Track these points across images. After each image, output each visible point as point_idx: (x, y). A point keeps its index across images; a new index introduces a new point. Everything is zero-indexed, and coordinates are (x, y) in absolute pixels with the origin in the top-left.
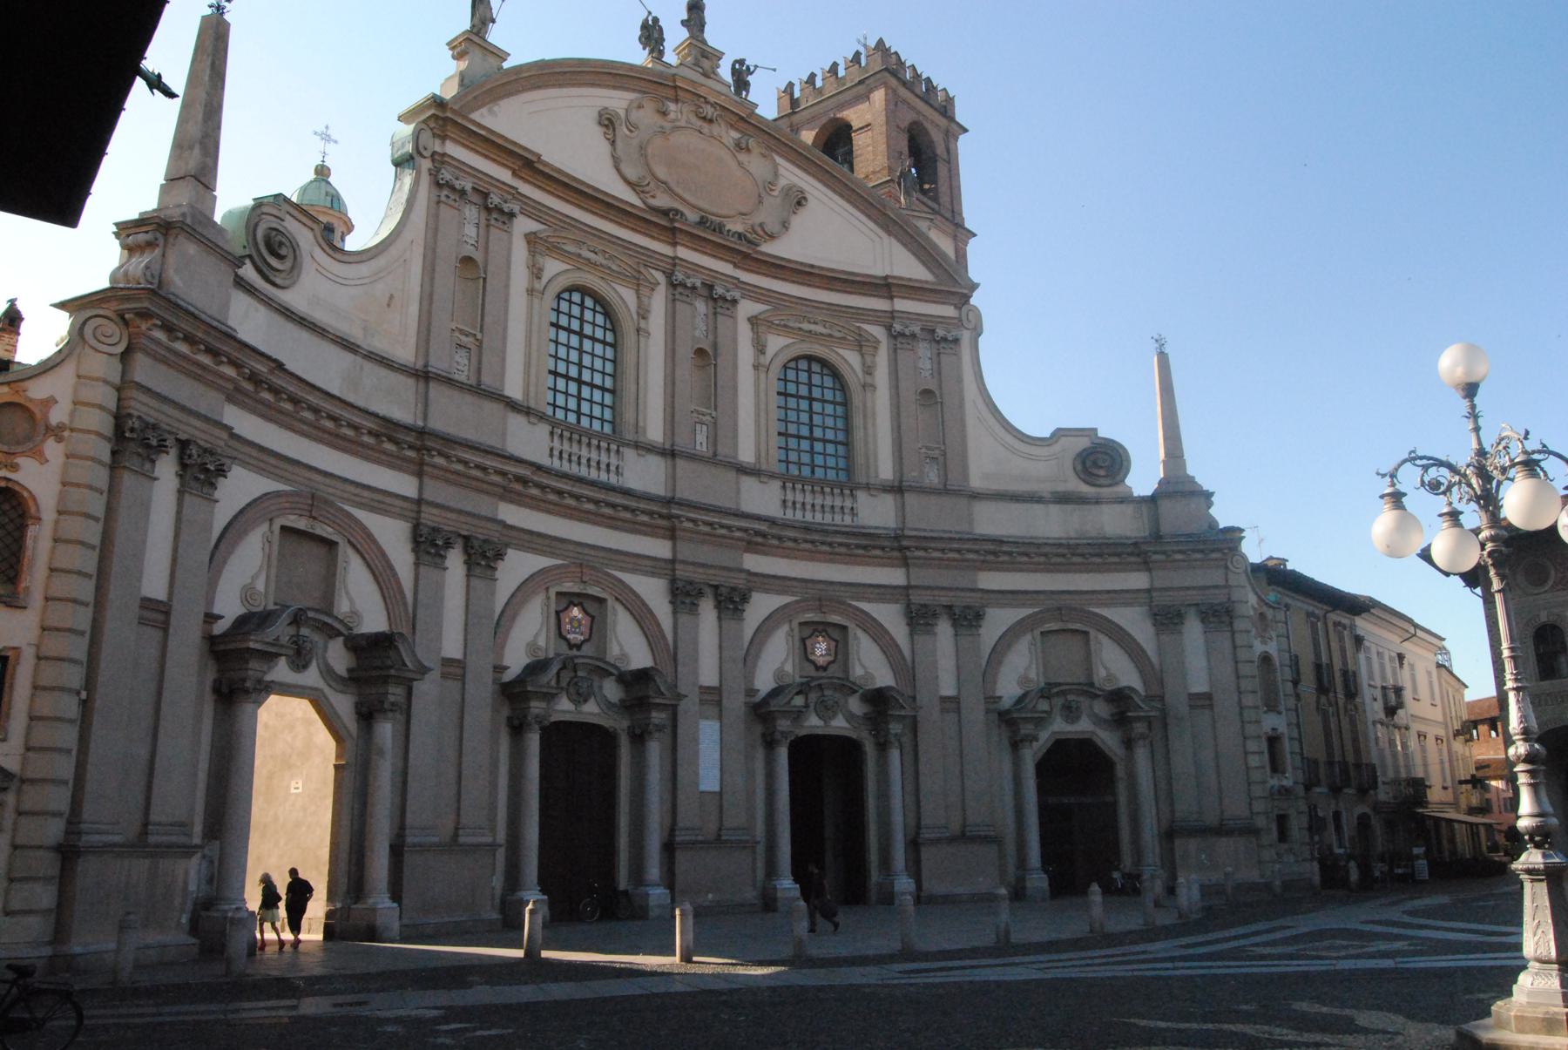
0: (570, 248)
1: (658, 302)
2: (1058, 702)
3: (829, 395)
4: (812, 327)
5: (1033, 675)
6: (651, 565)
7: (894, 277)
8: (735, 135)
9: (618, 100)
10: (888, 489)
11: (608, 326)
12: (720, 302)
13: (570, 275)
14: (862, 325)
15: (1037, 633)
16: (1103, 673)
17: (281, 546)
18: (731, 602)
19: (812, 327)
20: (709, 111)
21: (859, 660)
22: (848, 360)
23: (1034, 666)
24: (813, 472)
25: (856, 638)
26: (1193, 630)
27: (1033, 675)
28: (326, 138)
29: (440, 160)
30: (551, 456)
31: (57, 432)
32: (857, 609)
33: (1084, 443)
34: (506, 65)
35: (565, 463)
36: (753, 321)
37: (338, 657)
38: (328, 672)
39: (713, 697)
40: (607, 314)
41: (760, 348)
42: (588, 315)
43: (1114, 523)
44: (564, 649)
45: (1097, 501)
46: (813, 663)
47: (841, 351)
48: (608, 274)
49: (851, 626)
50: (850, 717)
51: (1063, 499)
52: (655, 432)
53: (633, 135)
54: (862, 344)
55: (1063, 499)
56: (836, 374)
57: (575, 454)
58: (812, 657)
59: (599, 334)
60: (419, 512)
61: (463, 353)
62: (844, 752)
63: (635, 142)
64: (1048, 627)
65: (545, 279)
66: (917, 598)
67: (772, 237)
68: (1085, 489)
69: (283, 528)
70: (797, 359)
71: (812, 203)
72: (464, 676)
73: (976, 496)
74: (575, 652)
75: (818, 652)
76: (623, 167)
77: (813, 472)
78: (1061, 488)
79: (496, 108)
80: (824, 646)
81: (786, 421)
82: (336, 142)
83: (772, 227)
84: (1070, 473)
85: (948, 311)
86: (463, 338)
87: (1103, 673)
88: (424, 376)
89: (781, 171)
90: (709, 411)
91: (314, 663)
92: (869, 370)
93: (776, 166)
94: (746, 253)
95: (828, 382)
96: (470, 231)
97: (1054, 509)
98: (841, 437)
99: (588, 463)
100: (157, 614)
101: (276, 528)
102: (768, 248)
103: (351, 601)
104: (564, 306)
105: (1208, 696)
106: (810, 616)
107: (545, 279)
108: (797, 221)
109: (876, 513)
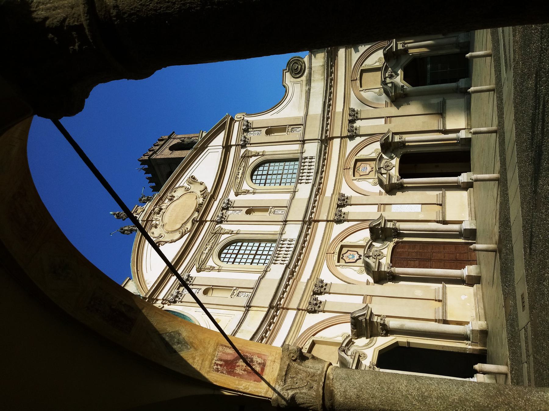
0: (204, 257)
1: (225, 227)
2: (388, 80)
3: (266, 168)
4: (240, 174)
7: (223, 144)
8: (167, 200)
11: (235, 244)
14: (240, 156)
18: (343, 202)
19: (240, 174)
20: (157, 209)
24: (295, 173)
30: (283, 264)
36: (237, 194)
42: (230, 251)
48: (215, 244)
52: (277, 228)
53: (163, 236)
54: (246, 157)
55: (309, 81)
57: (283, 255)
59: (238, 248)
60: (302, 310)
61: (240, 294)
63: (166, 234)
65: (215, 266)
67: (206, 188)
70: (252, 180)
71: (195, 174)
72: (370, 296)
73: (307, 114)
76: (175, 238)
77: (295, 173)
78: (304, 83)
83: (202, 188)
87: (377, 64)
89: (181, 185)
90: (270, 209)
91: (364, 351)
93: (179, 187)
95: (261, 168)
99: (286, 252)
104: (226, 260)
107: (215, 266)
109: (312, 149)
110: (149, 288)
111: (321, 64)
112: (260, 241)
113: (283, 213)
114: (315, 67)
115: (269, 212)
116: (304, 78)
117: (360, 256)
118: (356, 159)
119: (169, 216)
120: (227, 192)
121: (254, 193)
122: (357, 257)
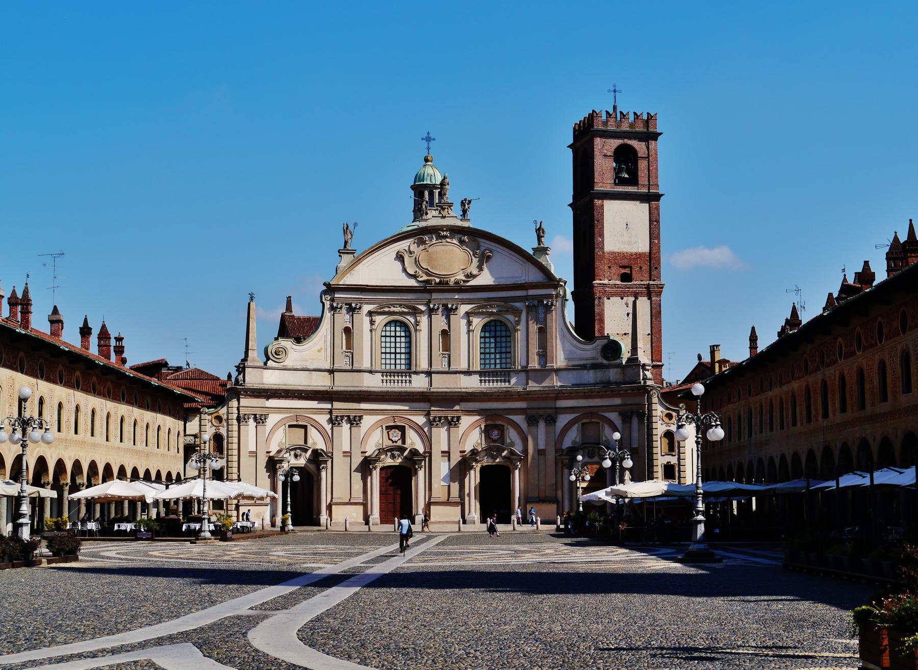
5: (578, 440)
9: (403, 245)
13: (387, 318)
15: (580, 423)
16: (604, 439)
17: (289, 430)
21: (509, 436)
23: (578, 437)
25: (507, 428)
27: (578, 440)
28: (428, 139)
30: (383, 382)
32: (507, 418)
33: (605, 341)
35: (385, 384)
43: (613, 374)
44: (390, 443)
45: (608, 367)
46: (492, 439)
47: (507, 316)
49: (506, 425)
51: (595, 367)
52: (424, 365)
55: (595, 367)
56: (506, 325)
58: (492, 437)
64: (585, 421)
65: (376, 324)
68: (605, 362)
69: (289, 425)
74: (395, 444)
75: (494, 435)
77: (495, 366)
78: (594, 361)
79: (352, 272)
80: (496, 432)
81: (485, 348)
82: (434, 139)
83: (475, 272)
84: (599, 355)
86: (346, 353)
87: (604, 439)
88: (331, 372)
89: (482, 244)
97: (592, 372)
98: (508, 350)
100: (254, 454)
101: (287, 426)
102: (473, 282)
103: (313, 440)
105: (636, 449)
110: (340, 283)
111: (611, 379)
112: (409, 353)
113: (443, 366)
114: (609, 372)
115: (443, 353)
116: (601, 360)
117: (396, 442)
118: (504, 426)
119: (436, 252)
120: (465, 301)
121: (469, 331)
122: (394, 439)
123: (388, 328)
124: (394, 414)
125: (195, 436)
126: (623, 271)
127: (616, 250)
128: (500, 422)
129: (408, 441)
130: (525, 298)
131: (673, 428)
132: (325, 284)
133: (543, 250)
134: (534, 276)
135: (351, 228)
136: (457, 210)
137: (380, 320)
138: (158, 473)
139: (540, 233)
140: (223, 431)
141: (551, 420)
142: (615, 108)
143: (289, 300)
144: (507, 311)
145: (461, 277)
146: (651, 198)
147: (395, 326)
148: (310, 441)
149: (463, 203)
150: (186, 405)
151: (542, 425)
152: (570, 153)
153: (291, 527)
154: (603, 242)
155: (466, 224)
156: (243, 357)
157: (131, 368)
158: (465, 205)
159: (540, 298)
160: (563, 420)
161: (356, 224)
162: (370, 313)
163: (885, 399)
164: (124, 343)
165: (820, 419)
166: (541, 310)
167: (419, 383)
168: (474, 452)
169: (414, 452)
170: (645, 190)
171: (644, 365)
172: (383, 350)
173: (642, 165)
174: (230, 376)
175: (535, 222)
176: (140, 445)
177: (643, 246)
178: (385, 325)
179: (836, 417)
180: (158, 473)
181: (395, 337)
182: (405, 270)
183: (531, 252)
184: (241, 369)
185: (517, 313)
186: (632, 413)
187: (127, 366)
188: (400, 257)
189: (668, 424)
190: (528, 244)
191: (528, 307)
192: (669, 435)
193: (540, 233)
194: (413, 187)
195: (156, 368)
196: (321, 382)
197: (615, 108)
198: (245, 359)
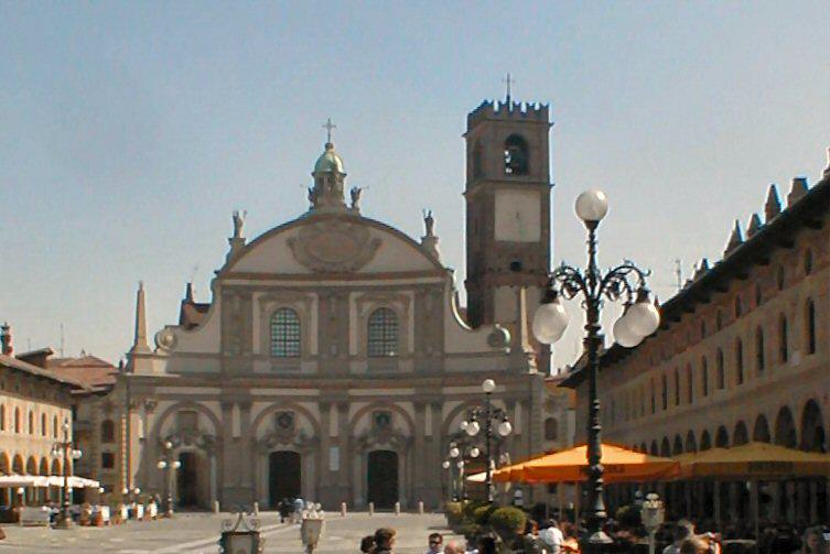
6: (313, 399)
9: (295, 232)
10: (411, 356)
12: (341, 295)
22: (399, 305)
26: (518, 408)
28: (329, 126)
29: (224, 287)
31: (116, 407)
34: (247, 242)
37: (200, 440)
38: (197, 445)
39: (335, 441)
40: (296, 314)
41: (359, 310)
50: (392, 444)
51: (480, 355)
52: (314, 350)
54: (406, 300)
62: (391, 457)
66: (418, 399)
68: (490, 349)
85: (438, 280)
92: (406, 309)
94: (349, 275)
96: (237, 306)
102: (363, 270)
106: (377, 409)
108: (379, 255)
116: (486, 348)
123: (278, 316)
124: (285, 400)
125: (86, 422)
126: (515, 260)
127: (506, 239)
128: (387, 409)
129: (298, 427)
130: (413, 286)
131: (556, 415)
132: (216, 272)
133: (430, 239)
134: (421, 263)
135: (241, 216)
136: (348, 201)
137: (271, 306)
138: (31, 460)
139: (429, 221)
140: (113, 417)
141: (438, 407)
142: (508, 98)
143: (189, 286)
144: (395, 299)
145: (349, 265)
146: (543, 186)
147: (285, 314)
148: (200, 428)
149: (352, 192)
150: (73, 392)
151: (428, 410)
152: (464, 141)
153: (171, 511)
154: (493, 231)
155: (353, 213)
156: (133, 344)
157: (16, 357)
158: (355, 194)
159: (427, 287)
160: (449, 407)
161: (245, 213)
162: (260, 299)
163: (722, 387)
164: (11, 332)
165: (673, 405)
166: (429, 297)
167: (308, 368)
168: (363, 439)
169: (303, 437)
170: (534, 180)
171: (528, 354)
172: (273, 337)
173: (534, 154)
174: (121, 363)
175: (424, 211)
176: (24, 430)
177: (533, 235)
178: (276, 313)
179: (672, 408)
180: (31, 460)
181: (285, 324)
182: (295, 256)
183: (420, 241)
184: (132, 355)
185: (406, 300)
186: (515, 400)
187: (13, 355)
188: (291, 243)
189: (550, 412)
190: (417, 233)
191: (416, 296)
192: (550, 421)
193: (429, 221)
194: (313, 174)
195: (39, 357)
196: (212, 366)
197: (508, 98)
198: (133, 349)
